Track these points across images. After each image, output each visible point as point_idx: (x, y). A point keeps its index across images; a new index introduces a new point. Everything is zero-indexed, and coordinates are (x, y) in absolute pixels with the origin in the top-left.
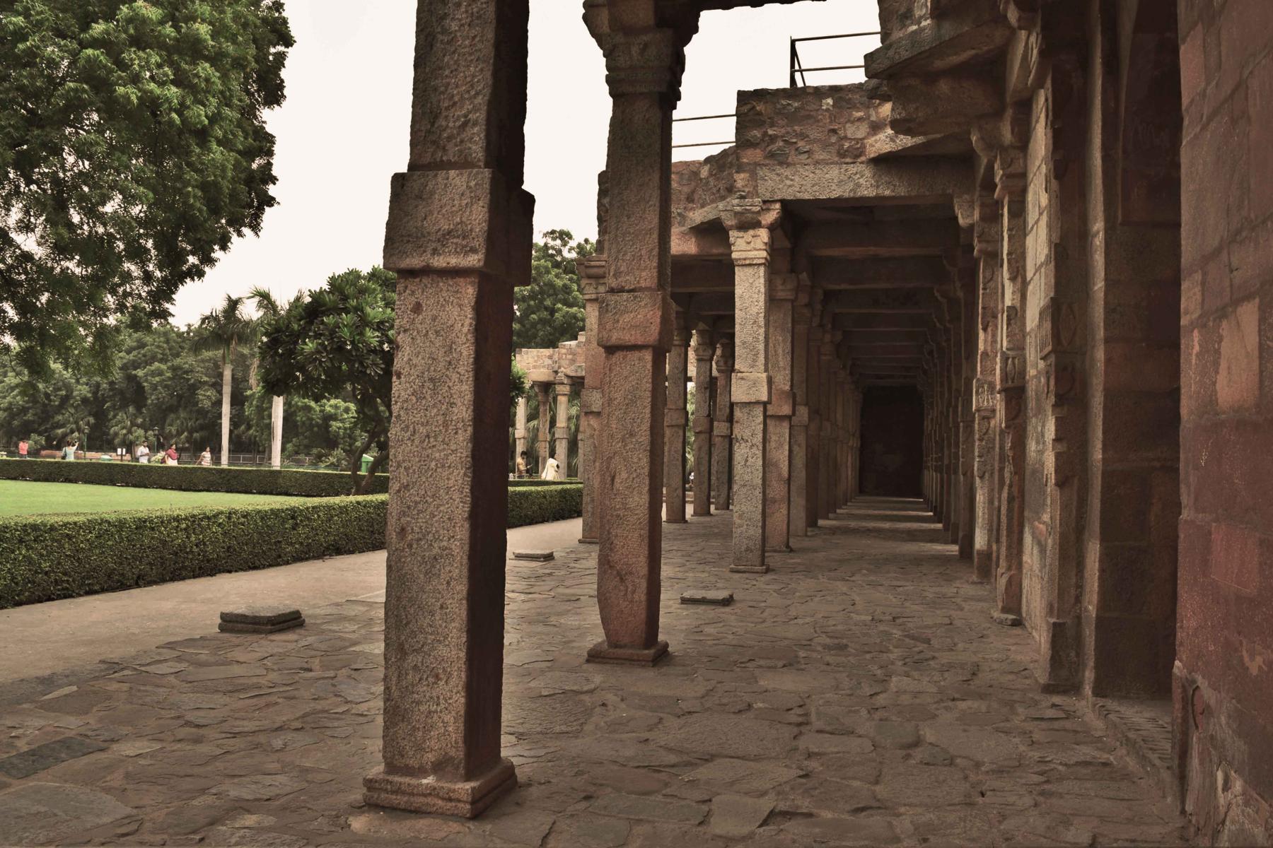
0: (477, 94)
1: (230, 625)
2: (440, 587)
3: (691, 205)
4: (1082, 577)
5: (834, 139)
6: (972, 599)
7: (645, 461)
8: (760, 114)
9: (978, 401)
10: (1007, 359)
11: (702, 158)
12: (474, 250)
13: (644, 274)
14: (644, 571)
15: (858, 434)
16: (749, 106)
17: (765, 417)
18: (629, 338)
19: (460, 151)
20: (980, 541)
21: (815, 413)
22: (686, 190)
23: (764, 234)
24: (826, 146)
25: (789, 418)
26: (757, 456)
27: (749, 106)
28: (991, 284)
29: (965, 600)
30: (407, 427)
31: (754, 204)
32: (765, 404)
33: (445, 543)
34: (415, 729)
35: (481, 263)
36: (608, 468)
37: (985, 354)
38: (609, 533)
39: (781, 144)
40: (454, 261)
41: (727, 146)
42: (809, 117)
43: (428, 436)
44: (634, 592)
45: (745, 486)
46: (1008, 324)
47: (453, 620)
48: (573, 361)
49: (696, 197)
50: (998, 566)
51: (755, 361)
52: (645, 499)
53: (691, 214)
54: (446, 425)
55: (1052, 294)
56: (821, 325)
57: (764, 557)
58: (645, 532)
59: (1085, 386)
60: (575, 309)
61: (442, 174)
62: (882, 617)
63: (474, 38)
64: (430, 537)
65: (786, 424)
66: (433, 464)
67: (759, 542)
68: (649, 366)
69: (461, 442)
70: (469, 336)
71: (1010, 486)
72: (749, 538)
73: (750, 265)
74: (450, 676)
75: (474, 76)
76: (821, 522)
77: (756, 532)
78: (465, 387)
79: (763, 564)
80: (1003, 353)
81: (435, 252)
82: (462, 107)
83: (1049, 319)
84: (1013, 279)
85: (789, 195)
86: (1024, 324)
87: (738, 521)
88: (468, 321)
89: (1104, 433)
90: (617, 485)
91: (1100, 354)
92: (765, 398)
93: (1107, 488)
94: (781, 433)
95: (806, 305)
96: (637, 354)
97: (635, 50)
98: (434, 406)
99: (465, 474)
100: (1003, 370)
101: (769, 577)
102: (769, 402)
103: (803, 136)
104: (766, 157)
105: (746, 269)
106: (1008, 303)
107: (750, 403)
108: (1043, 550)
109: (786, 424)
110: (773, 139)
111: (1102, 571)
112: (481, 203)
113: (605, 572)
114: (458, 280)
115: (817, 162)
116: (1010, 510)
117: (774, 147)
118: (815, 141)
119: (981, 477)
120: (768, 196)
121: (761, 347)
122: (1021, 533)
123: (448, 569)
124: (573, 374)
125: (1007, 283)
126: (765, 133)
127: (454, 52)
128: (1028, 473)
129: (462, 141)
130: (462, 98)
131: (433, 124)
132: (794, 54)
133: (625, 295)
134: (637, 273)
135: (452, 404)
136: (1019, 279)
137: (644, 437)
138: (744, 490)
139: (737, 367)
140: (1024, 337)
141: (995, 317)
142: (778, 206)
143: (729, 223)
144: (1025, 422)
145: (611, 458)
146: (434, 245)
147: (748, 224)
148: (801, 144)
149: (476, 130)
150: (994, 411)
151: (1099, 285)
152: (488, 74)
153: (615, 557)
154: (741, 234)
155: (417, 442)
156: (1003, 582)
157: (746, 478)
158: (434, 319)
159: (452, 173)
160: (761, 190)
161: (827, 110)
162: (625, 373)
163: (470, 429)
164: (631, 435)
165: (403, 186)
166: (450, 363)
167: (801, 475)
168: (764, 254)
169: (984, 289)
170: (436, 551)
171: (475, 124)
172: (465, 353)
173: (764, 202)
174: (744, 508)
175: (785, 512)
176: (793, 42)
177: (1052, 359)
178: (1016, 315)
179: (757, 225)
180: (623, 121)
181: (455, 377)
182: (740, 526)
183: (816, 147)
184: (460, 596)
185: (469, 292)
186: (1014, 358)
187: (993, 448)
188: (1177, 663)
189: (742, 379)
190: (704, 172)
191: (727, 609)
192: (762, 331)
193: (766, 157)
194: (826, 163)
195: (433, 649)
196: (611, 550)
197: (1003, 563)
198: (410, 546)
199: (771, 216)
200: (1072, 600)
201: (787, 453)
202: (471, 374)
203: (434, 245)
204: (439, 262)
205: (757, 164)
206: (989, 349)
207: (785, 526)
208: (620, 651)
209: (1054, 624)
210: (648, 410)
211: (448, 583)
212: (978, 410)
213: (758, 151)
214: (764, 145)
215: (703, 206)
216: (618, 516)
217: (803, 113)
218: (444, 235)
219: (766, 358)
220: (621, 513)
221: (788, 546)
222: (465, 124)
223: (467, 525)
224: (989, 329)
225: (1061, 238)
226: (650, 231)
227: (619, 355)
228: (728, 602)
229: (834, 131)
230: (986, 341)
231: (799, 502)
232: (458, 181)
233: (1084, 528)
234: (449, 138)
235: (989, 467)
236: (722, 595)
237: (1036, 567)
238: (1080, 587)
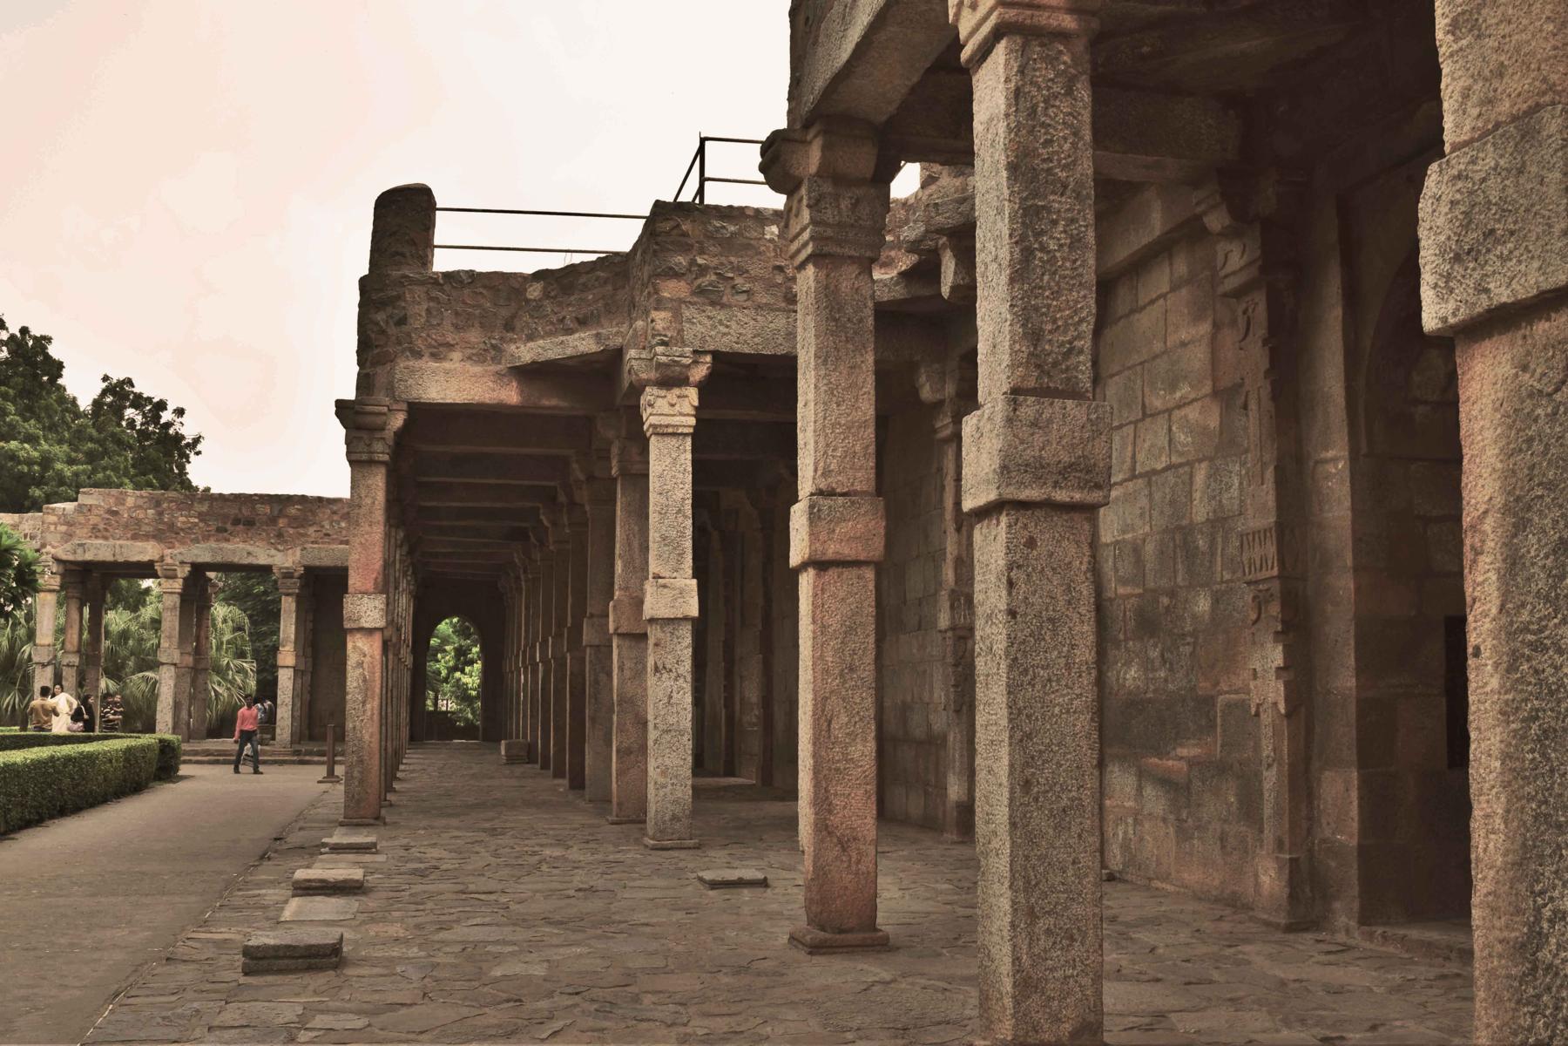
0: (1081, 321)
1: (265, 963)
3: (509, 335)
5: (779, 279)
7: (869, 702)
8: (685, 234)
11: (530, 270)
16: (672, 223)
18: (848, 551)
19: (1068, 379)
22: (504, 313)
23: (693, 394)
24: (770, 286)
27: (672, 223)
30: (1026, 671)
31: (684, 355)
34: (1050, 999)
38: (827, 791)
39: (714, 278)
40: (1077, 496)
41: (577, 259)
42: (748, 247)
43: (1050, 680)
44: (858, 862)
47: (1086, 875)
48: (68, 536)
49: (518, 325)
53: (513, 347)
54: (1068, 667)
58: (872, 788)
60: (14, 444)
61: (1058, 402)
63: (1075, 261)
64: (1058, 788)
66: (1057, 710)
68: (871, 586)
72: (676, 802)
73: (674, 434)
74: (1085, 936)
75: (1077, 302)
78: (1086, 628)
81: (1056, 484)
82: (1065, 332)
85: (725, 344)
91: (1344, 584)
96: (855, 572)
97: (845, 204)
98: (1055, 647)
103: (741, 271)
104: (693, 293)
105: (667, 440)
110: (703, 270)
111: (1361, 798)
113: (822, 841)
115: (759, 307)
117: (705, 281)
118: (753, 279)
120: (697, 345)
124: (71, 558)
126: (693, 262)
127: (1055, 273)
129: (1068, 369)
130: (1066, 325)
131: (1035, 346)
132: (701, 152)
133: (840, 500)
134: (850, 473)
135: (1073, 646)
138: (668, 737)
142: (708, 358)
143: (644, 376)
145: (826, 699)
146: (1055, 477)
147: (671, 380)
148: (739, 280)
149: (1082, 358)
152: (1092, 302)
153: (835, 820)
154: (663, 393)
155: (1038, 687)
157: (672, 720)
158: (1051, 555)
159: (1069, 403)
160: (688, 336)
161: (771, 241)
162: (841, 594)
164: (851, 670)
165: (1015, 410)
168: (692, 421)
170: (1065, 802)
171: (1081, 352)
173: (695, 352)
174: (668, 762)
176: (703, 141)
179: (683, 382)
180: (827, 287)
181: (1075, 617)
183: (757, 287)
189: (665, 586)
190: (535, 291)
193: (693, 293)
194: (770, 308)
195: (1066, 908)
196: (830, 812)
198: (1036, 800)
199: (700, 372)
203: (1055, 477)
204: (1061, 496)
205: (681, 301)
208: (850, 936)
210: (872, 639)
213: (682, 283)
214: (691, 276)
215: (531, 338)
216: (837, 770)
217: (741, 240)
220: (841, 766)
222: (1070, 351)
226: (864, 424)
227: (832, 573)
229: (780, 269)
232: (1075, 412)
234: (1055, 364)
236: (760, 876)
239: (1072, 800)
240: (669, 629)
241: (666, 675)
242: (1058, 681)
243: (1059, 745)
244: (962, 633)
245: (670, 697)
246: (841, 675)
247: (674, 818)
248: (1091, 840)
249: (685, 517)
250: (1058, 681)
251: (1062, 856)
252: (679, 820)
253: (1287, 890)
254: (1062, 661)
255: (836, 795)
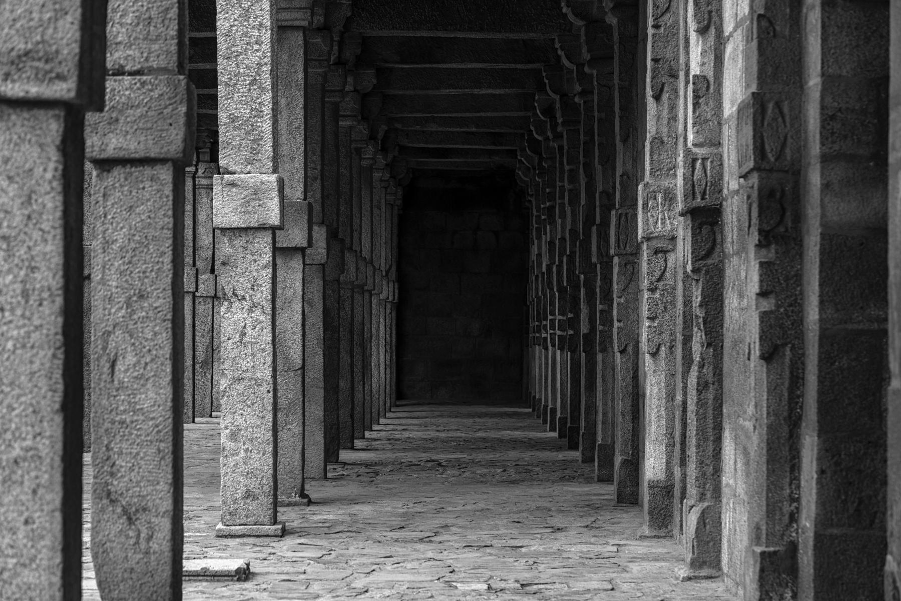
2: (23, 498)
4: (799, 487)
6: (645, 558)
7: (165, 339)
9: (646, 223)
10: (694, 161)
12: (60, 77)
13: (156, 47)
14: (167, 505)
15: (393, 274)
17: (276, 250)
20: (653, 465)
21: (333, 236)
25: (302, 250)
26: (255, 326)
28: (668, 19)
29: (633, 560)
32: (274, 229)
33: (28, 443)
35: (72, 94)
36: (104, 348)
37: (658, 141)
38: (108, 448)
40: (34, 90)
44: (150, 538)
45: (240, 379)
46: (696, 105)
47: (42, 537)
50: (683, 496)
51: (255, 152)
52: (167, 392)
54: (25, 294)
55: (754, 88)
56: (339, 62)
57: (284, 503)
59: (799, 218)
62: (503, 585)
65: (296, 264)
66: (10, 345)
67: (268, 481)
68: (168, 190)
69: (49, 317)
70: (55, 184)
71: (701, 366)
76: (345, 455)
77: (262, 463)
78: (49, 248)
79: (275, 523)
80: (688, 152)
83: (750, 122)
84: (703, 31)
86: (719, 106)
87: (230, 445)
88: (52, 165)
89: (821, 285)
90: (119, 375)
92: (274, 218)
93: (825, 359)
94: (293, 277)
95: (319, 29)
96: (148, 171)
98: (9, 271)
99: (54, 356)
100: (690, 181)
101: (290, 541)
102: (281, 228)
106: (695, 70)
107: (246, 229)
108: (746, 452)
109: (296, 264)
112: (69, 18)
113: (103, 510)
114: (35, 112)
116: (701, 403)
119: (655, 354)
121: (266, 126)
122: (719, 440)
123: (33, 474)
125: (693, 36)
128: (727, 344)
133: (127, 78)
135: (33, 269)
136: (712, 30)
137: (162, 300)
138: (240, 387)
139: (222, 163)
140: (720, 124)
141: (675, 76)
144: (721, 261)
145: (109, 333)
150: (673, 239)
151: (814, 82)
153: (117, 485)
156: (692, 520)
157: (244, 364)
163: (59, 301)
164: (141, 297)
166: (29, 217)
167: (317, 361)
169: (656, 26)
170: (17, 452)
172: (50, 205)
174: (240, 421)
175: (296, 428)
177: (754, 179)
178: (707, 89)
181: (36, 235)
182: (235, 453)
184: (51, 507)
185: (53, 127)
186: (704, 159)
187: (673, 303)
188: (889, 558)
189: (233, 184)
191: (248, 585)
192: (268, 96)
195: (16, 575)
197: (692, 491)
200: (786, 519)
201: (298, 318)
202: (59, 232)
206: (665, 131)
207: (298, 456)
209: (763, 554)
211: (34, 492)
212: (648, 239)
216: (122, 422)
218: (19, 57)
219: (276, 146)
220: (127, 418)
221: (303, 495)
223: (59, 419)
224: (665, 97)
225: (767, 8)
227: (118, 173)
228: (244, 574)
230: (659, 118)
231: (316, 410)
233: (800, 418)
235: (666, 336)
236: (233, 564)
237: (741, 489)
238: (795, 500)
239: (28, 450)
240: (239, 242)
241: (237, 305)
242: (12, 310)
243: (12, 384)
244: (660, 244)
245: (243, 334)
246: (128, 304)
247: (249, 495)
248: (49, 497)
249: (262, 89)
250: (12, 310)
251: (11, 516)
252: (255, 498)
253: (758, 593)
254: (18, 287)
255: (120, 453)
